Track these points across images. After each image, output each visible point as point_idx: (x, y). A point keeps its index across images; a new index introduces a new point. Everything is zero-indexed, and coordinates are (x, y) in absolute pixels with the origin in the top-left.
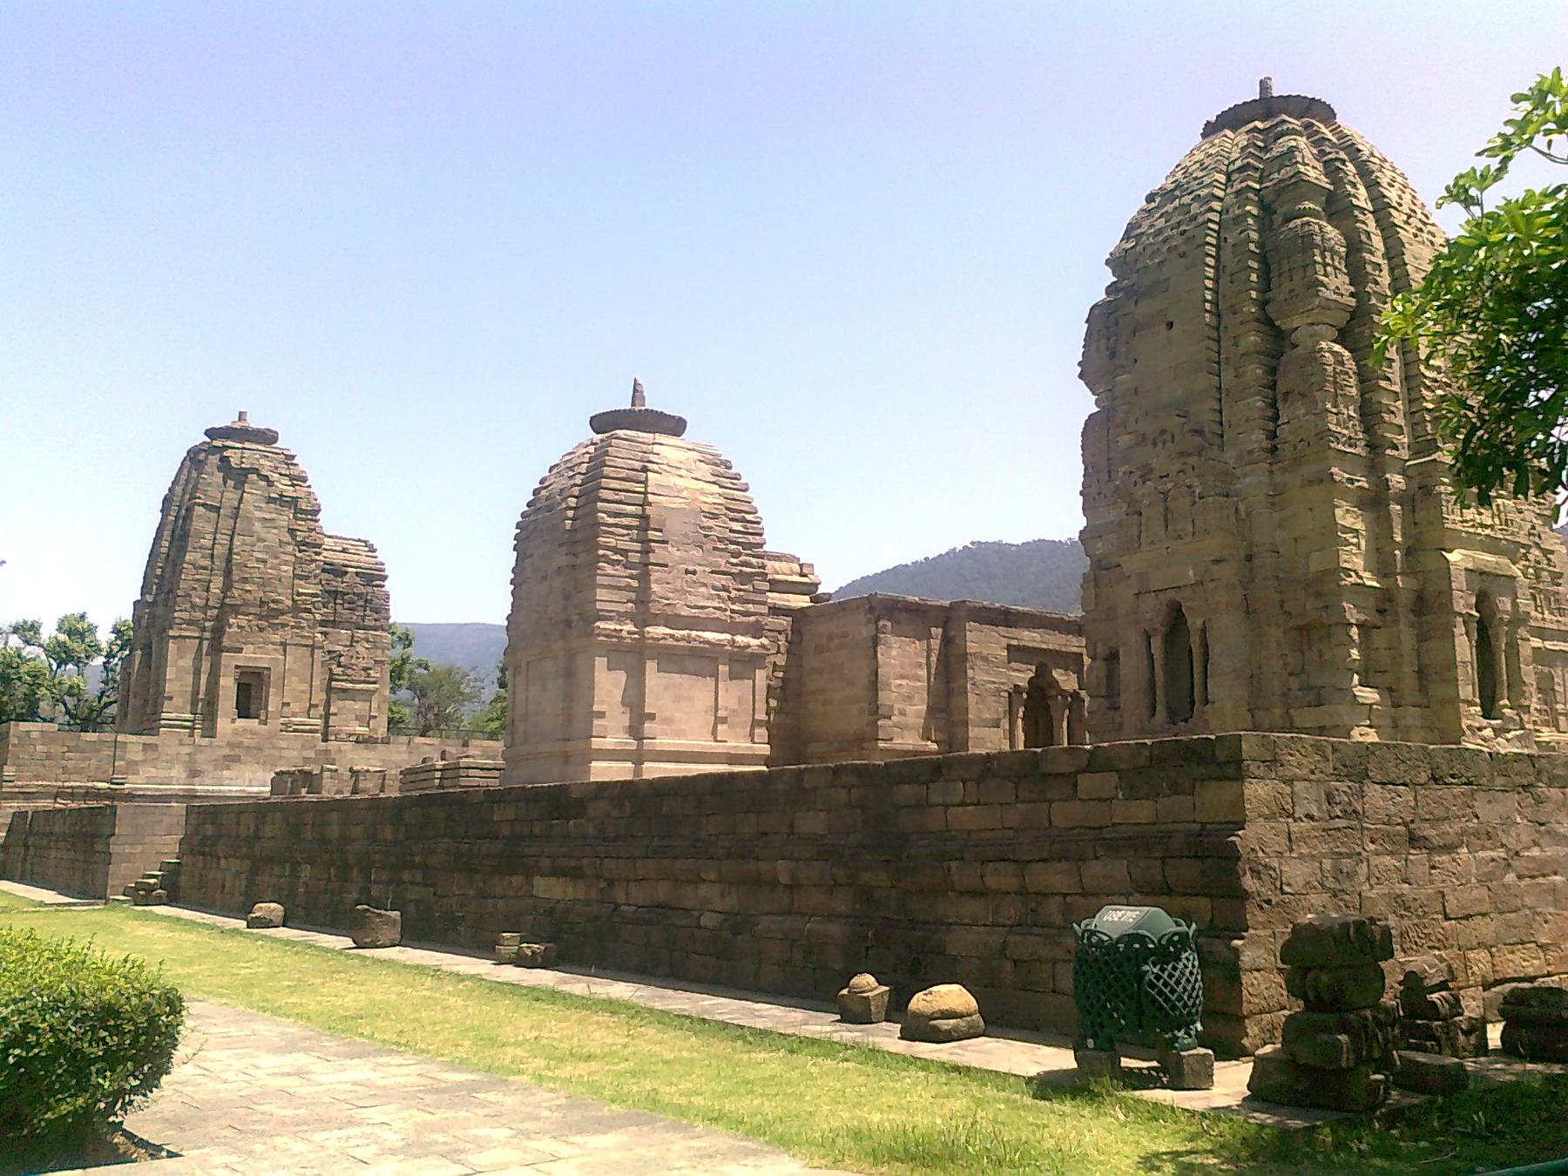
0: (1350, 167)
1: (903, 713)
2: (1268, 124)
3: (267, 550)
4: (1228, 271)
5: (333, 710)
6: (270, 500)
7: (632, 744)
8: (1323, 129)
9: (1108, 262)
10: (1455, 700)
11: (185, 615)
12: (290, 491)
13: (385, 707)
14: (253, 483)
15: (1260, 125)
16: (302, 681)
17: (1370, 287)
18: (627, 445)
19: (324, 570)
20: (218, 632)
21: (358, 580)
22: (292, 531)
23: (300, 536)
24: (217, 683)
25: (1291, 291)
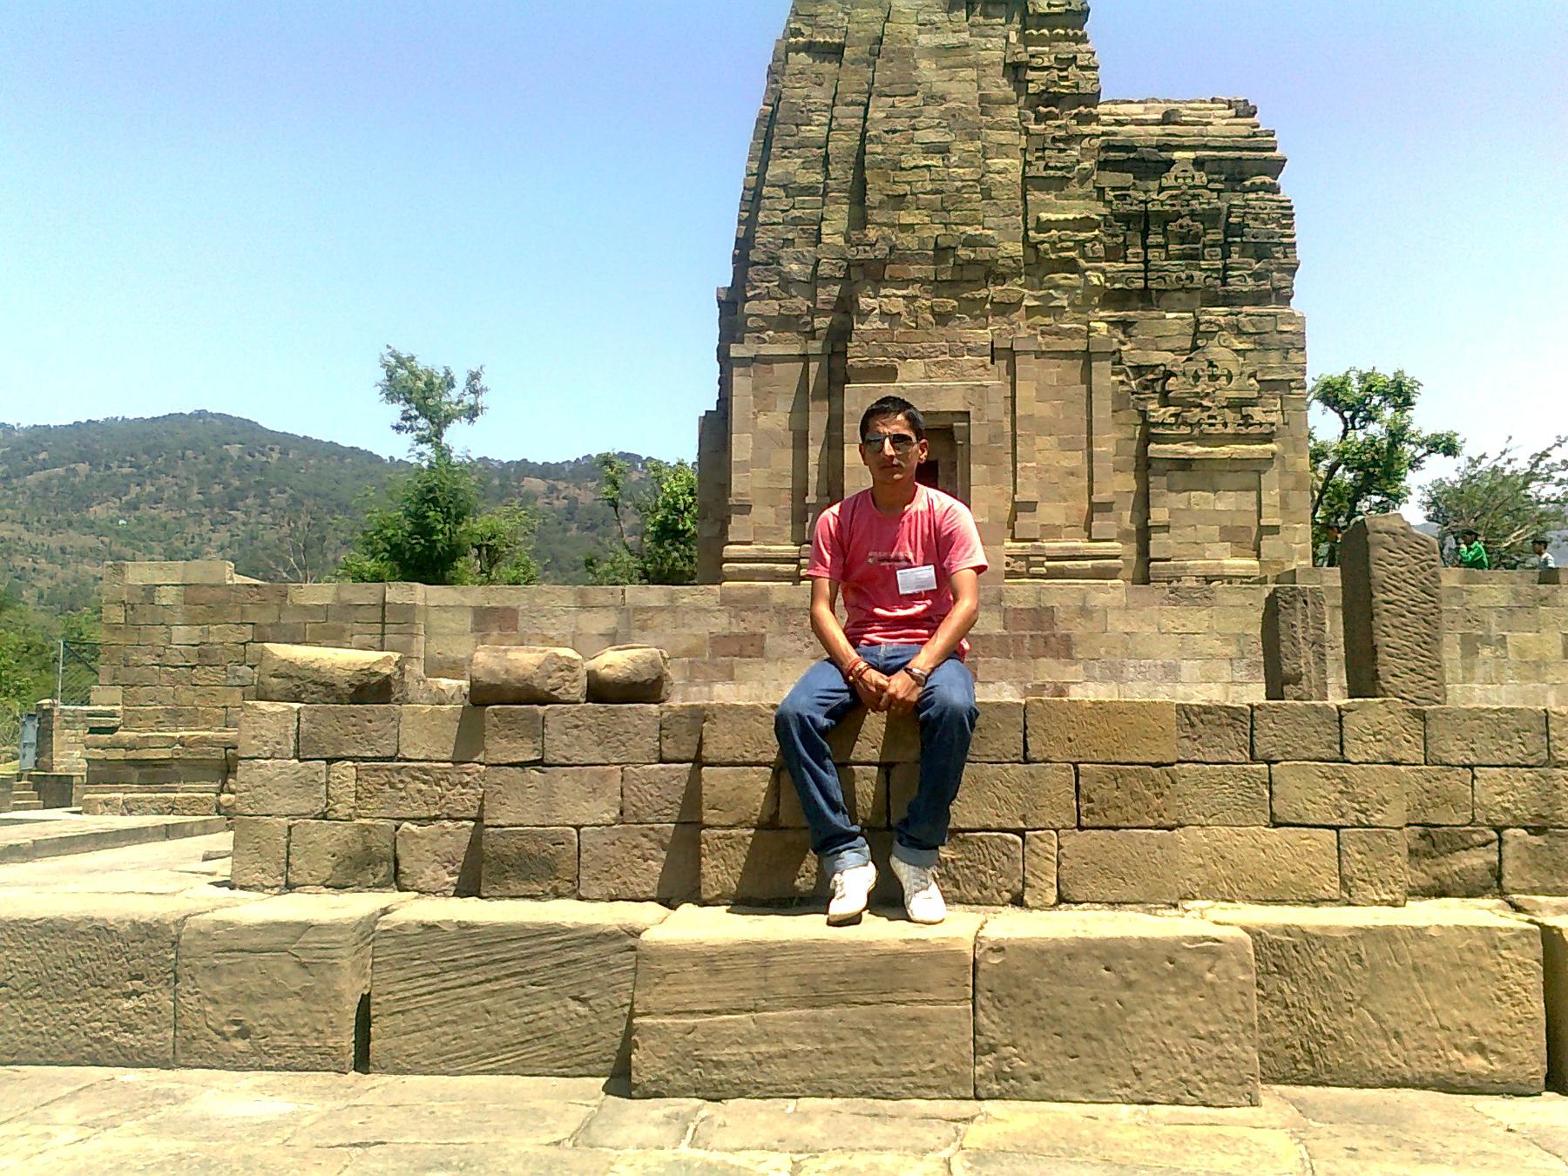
5: (1158, 515)
11: (771, 308)
13: (1303, 502)
16: (1066, 446)
19: (1103, 165)
20: (840, 336)
21: (1201, 178)
22: (1015, 71)
23: (1037, 81)
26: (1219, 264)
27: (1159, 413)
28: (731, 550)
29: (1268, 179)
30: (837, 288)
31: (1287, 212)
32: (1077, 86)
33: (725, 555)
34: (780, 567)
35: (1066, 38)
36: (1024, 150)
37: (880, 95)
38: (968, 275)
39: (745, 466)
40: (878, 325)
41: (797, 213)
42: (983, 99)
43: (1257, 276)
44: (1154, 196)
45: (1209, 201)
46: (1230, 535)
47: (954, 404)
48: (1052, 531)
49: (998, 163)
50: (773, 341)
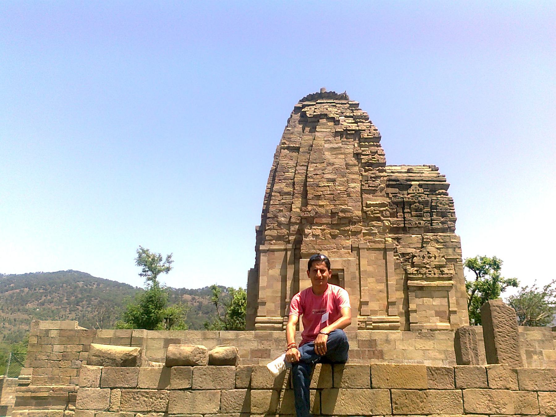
3: (337, 171)
5: (412, 306)
6: (337, 134)
11: (274, 233)
12: (354, 127)
13: (464, 302)
14: (323, 124)
16: (378, 281)
19: (388, 186)
20: (298, 243)
21: (421, 190)
22: (357, 156)
23: (364, 159)
26: (429, 219)
28: (258, 319)
29: (444, 191)
30: (297, 226)
31: (451, 202)
32: (378, 161)
33: (256, 321)
34: (276, 325)
35: (374, 145)
36: (361, 181)
37: (312, 163)
38: (342, 222)
39: (264, 288)
40: (312, 239)
41: (283, 201)
42: (347, 165)
43: (442, 223)
44: (406, 196)
46: (438, 314)
48: (374, 312)
49: (352, 185)
50: (275, 244)
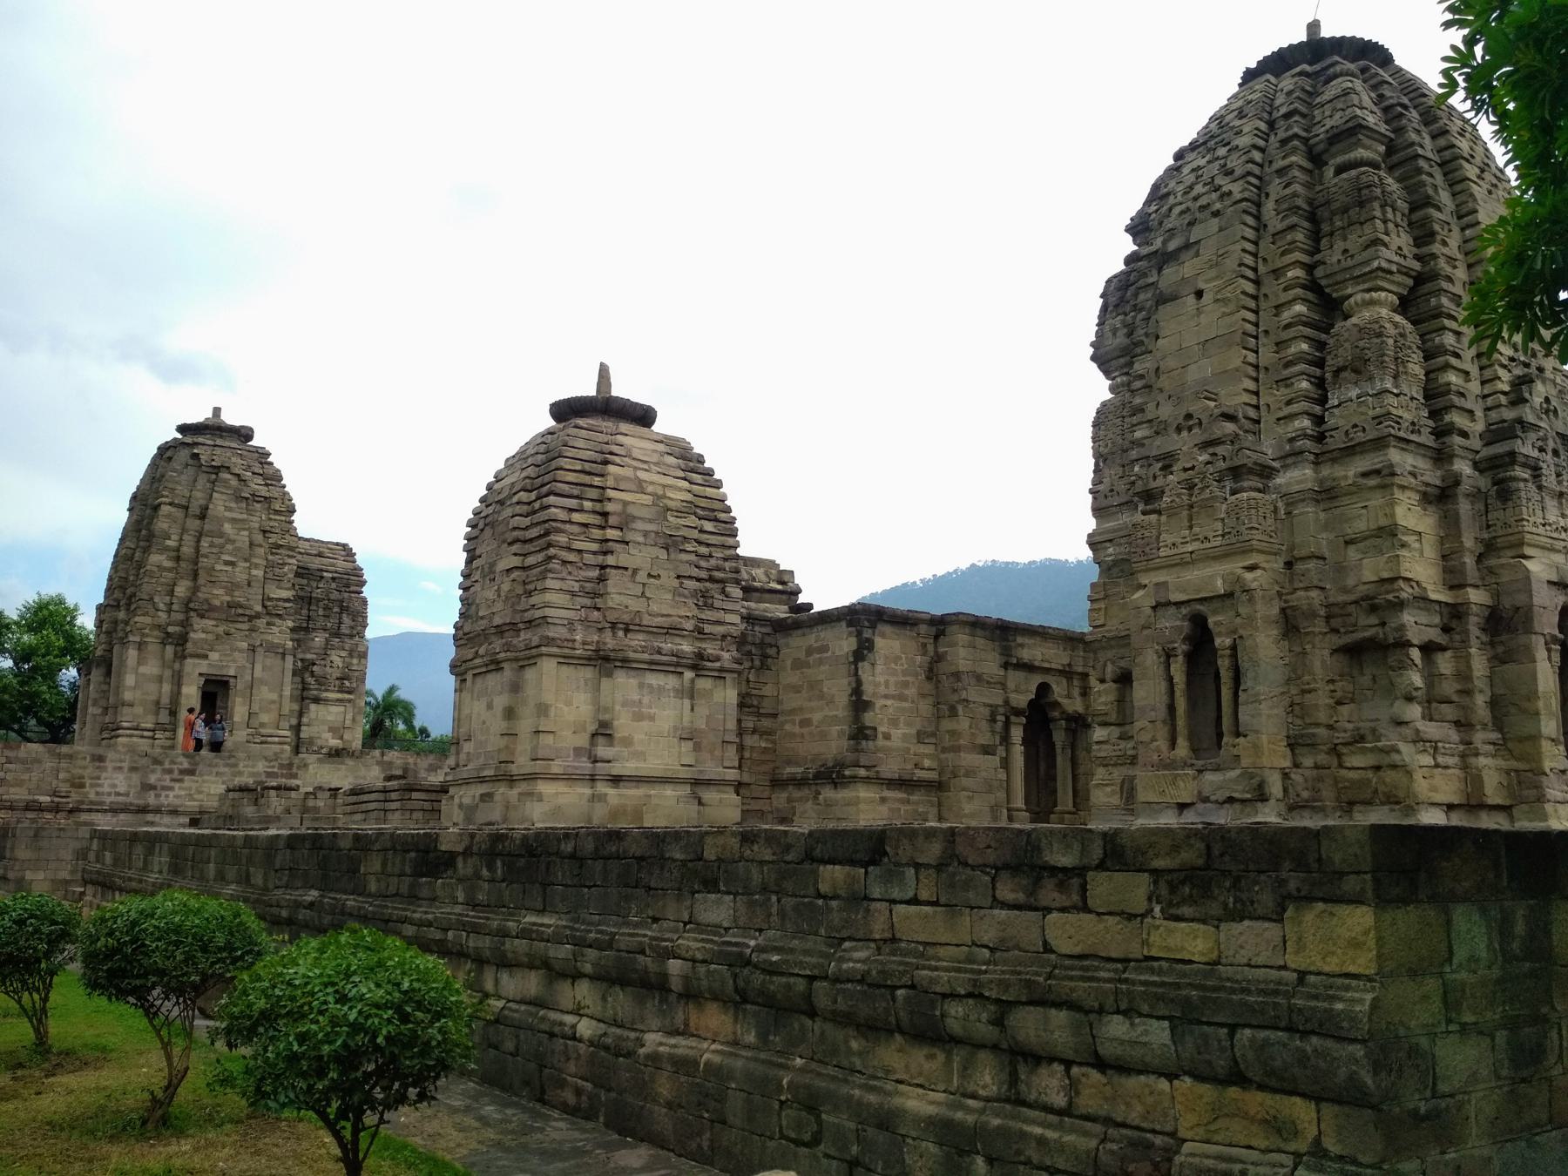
0: (1414, 114)
1: (887, 737)
2: (1317, 67)
4: (1271, 229)
7: (585, 765)
8: (1381, 71)
9: (1129, 230)
10: (1535, 738)
12: (263, 491)
14: (226, 481)
15: (1306, 67)
17: (1436, 248)
18: (585, 437)
24: (179, 693)
25: (1346, 251)
27: (310, 680)
42: (251, 544)
45: (335, 595)
47: (232, 673)
